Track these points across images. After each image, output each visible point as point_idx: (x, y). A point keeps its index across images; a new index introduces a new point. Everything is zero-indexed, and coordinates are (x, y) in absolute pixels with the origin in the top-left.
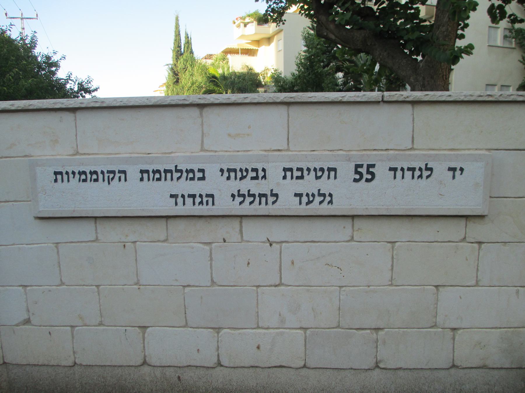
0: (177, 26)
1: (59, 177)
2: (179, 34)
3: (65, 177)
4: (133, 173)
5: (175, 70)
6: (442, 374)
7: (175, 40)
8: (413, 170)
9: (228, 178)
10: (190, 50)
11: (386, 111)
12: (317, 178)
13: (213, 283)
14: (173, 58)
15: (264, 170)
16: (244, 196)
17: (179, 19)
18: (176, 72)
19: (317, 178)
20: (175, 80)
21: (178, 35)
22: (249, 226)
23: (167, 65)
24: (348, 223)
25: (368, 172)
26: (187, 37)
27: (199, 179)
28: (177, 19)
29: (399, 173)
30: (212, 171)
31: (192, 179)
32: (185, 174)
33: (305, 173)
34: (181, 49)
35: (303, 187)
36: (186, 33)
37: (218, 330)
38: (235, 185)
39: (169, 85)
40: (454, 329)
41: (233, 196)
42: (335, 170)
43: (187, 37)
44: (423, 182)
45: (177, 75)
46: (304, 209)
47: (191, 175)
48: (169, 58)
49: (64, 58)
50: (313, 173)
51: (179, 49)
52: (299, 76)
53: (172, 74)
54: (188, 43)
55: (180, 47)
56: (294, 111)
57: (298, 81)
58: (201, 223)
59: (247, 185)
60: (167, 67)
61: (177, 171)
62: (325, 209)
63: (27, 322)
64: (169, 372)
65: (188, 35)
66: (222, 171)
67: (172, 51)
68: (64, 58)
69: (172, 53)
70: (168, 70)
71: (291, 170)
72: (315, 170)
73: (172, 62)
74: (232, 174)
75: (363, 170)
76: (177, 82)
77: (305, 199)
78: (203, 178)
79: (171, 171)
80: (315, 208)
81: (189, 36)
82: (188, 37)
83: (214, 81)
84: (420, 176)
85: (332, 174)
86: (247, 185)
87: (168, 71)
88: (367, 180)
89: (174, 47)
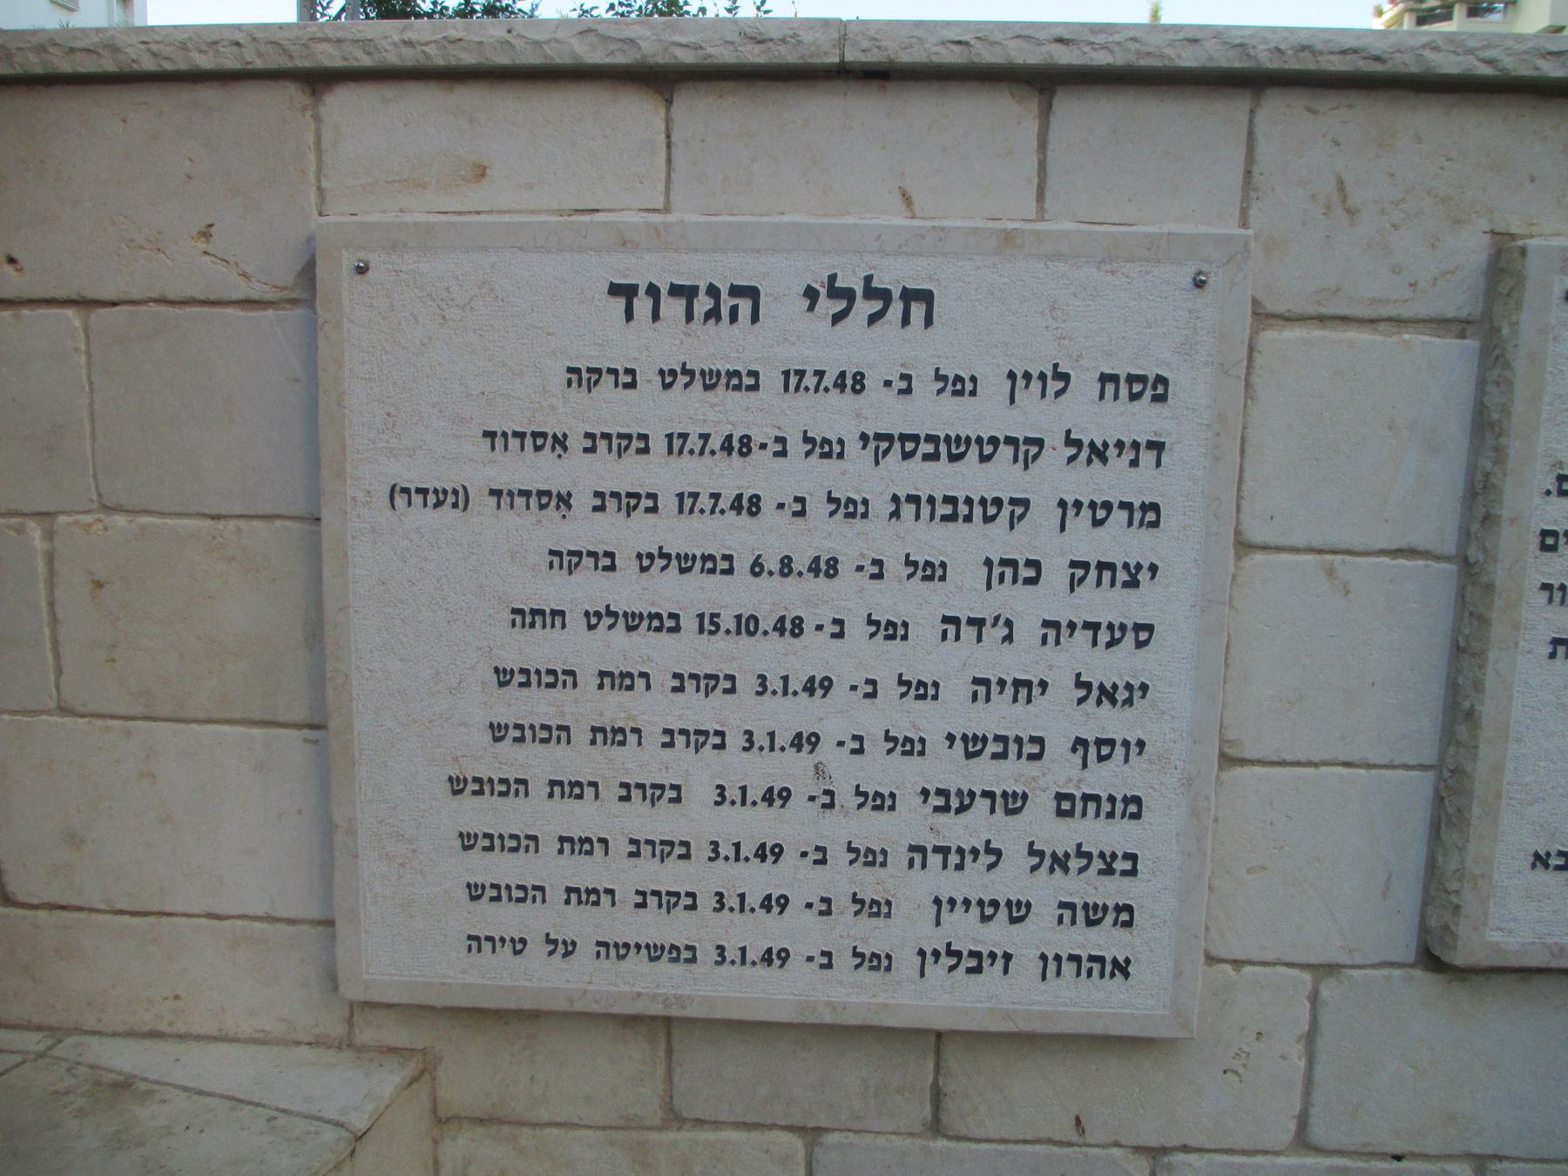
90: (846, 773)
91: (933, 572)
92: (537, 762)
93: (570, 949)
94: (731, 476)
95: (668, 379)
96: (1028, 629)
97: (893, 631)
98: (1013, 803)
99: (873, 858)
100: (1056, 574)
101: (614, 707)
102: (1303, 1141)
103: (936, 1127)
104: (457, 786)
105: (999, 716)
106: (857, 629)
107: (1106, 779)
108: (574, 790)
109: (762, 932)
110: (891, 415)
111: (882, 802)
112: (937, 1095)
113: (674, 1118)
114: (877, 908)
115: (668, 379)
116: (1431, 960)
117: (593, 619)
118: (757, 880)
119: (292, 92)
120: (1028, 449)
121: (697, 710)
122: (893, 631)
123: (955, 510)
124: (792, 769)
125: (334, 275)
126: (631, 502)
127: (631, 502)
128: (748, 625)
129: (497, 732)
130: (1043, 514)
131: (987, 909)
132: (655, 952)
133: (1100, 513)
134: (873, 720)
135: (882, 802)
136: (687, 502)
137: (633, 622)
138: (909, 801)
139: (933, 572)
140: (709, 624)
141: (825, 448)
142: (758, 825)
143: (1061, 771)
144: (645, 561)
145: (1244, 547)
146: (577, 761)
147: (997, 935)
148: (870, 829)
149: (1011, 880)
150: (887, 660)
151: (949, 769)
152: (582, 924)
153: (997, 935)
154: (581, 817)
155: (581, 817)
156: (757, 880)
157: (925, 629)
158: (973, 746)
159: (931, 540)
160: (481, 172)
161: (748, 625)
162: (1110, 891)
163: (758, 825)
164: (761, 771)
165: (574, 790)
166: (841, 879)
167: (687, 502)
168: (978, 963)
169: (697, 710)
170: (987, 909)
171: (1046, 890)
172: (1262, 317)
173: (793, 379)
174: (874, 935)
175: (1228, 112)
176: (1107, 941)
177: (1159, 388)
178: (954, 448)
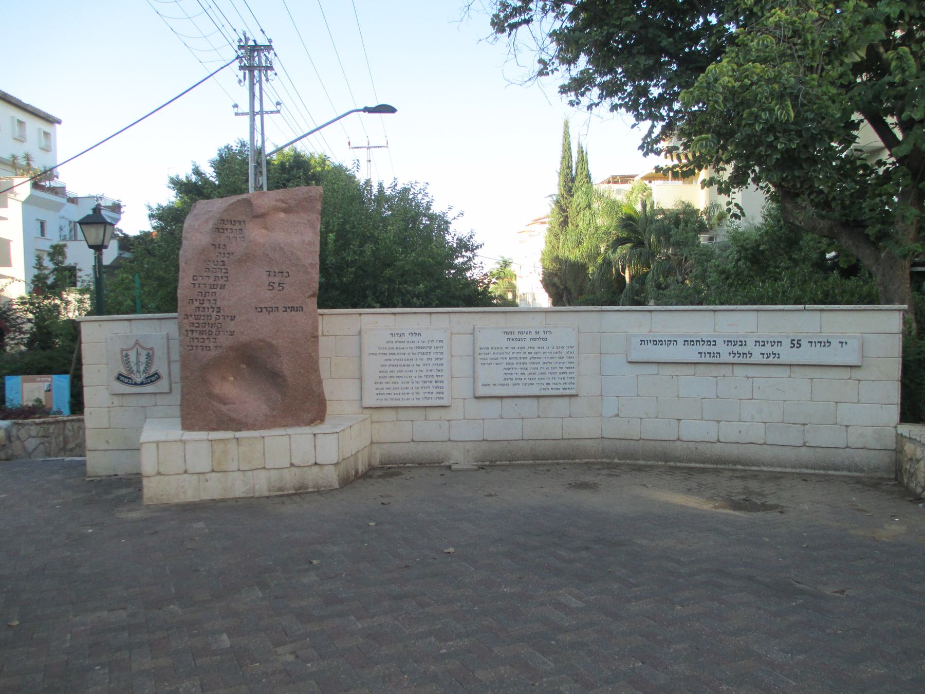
0: (566, 135)
1: (643, 343)
2: (570, 149)
3: (646, 342)
4: (680, 341)
5: (563, 203)
6: (840, 451)
7: (563, 158)
8: (820, 342)
9: (728, 345)
10: (585, 173)
11: (807, 314)
12: (772, 346)
13: (718, 397)
14: (559, 185)
15: (745, 341)
16: (735, 354)
17: (569, 124)
18: (564, 207)
19: (772, 346)
20: (562, 219)
21: (567, 149)
22: (737, 370)
23: (551, 196)
24: (788, 369)
25: (798, 343)
26: (581, 152)
27: (713, 345)
28: (566, 125)
29: (813, 344)
30: (720, 341)
31: (710, 345)
32: (706, 343)
33: (766, 343)
34: (571, 171)
35: (763, 350)
36: (579, 144)
37: (719, 422)
38: (731, 348)
39: (552, 227)
40: (847, 426)
41: (730, 353)
42: (781, 342)
43: (581, 152)
44: (826, 349)
45: (565, 211)
46: (765, 361)
47: (709, 343)
48: (553, 185)
49: (462, 214)
50: (770, 344)
51: (568, 171)
52: (767, 232)
53: (557, 210)
54: (583, 160)
55: (570, 167)
56: (760, 314)
57: (766, 238)
58: (712, 367)
59: (737, 349)
60: (550, 198)
61: (702, 341)
62: (776, 361)
63: (617, 415)
64: (691, 445)
65: (582, 148)
66: (724, 341)
67: (557, 174)
68: (462, 214)
69: (558, 178)
70: (551, 203)
71: (759, 342)
72: (771, 342)
73: (557, 192)
74: (730, 343)
75: (795, 342)
76: (565, 223)
77: (765, 356)
78: (715, 345)
79: (699, 341)
80: (771, 360)
81: (584, 149)
82: (582, 152)
83: (631, 225)
84: (825, 346)
85: (779, 344)
86: (737, 349)
87: (550, 205)
88: (797, 347)
89: (561, 169)
90: (415, 380)
91: (422, 360)
92: (383, 380)
93: (387, 399)
94: (402, 351)
95: (396, 342)
96: (431, 364)
97: (419, 365)
98: (431, 382)
99: (418, 388)
100: (434, 359)
101: (391, 374)
102: (464, 419)
103: (426, 419)
104: (375, 383)
105: (429, 373)
106: (415, 365)
107: (440, 379)
108: (387, 383)
109: (406, 397)
110: (418, 345)
111: (418, 383)
112: (426, 415)
113: (398, 420)
114: (418, 393)
115: (396, 342)
116: (476, 398)
117: (389, 366)
118: (406, 391)
119: (358, 315)
120: (430, 348)
121: (399, 374)
122: (419, 365)
123: (423, 354)
124: (409, 380)
125: (363, 333)
126: (393, 354)
127: (393, 354)
128: (404, 365)
129: (380, 377)
130: (432, 354)
131: (429, 393)
132: (396, 399)
133: (437, 353)
134: (417, 374)
135: (418, 383)
136: (398, 354)
137: (393, 366)
138: (421, 382)
139: (422, 360)
140: (401, 366)
141: (411, 348)
142: (407, 385)
143: (435, 378)
144: (394, 360)
145: (452, 356)
146: (387, 380)
147: (430, 396)
148: (417, 385)
149: (431, 390)
150: (418, 368)
151: (424, 379)
152: (389, 397)
153: (430, 396)
154: (388, 386)
155: (388, 386)
156: (406, 391)
157: (421, 365)
158: (427, 376)
159: (421, 356)
160: (377, 323)
161: (404, 365)
162: (441, 390)
163: (407, 385)
164: (406, 380)
165: (387, 383)
166: (415, 390)
167: (398, 354)
168: (429, 398)
169: (399, 374)
170: (429, 393)
171: (435, 391)
172: (452, 334)
173: (408, 342)
174: (418, 396)
175: (448, 315)
176: (441, 396)
177: (442, 341)
178: (423, 348)
